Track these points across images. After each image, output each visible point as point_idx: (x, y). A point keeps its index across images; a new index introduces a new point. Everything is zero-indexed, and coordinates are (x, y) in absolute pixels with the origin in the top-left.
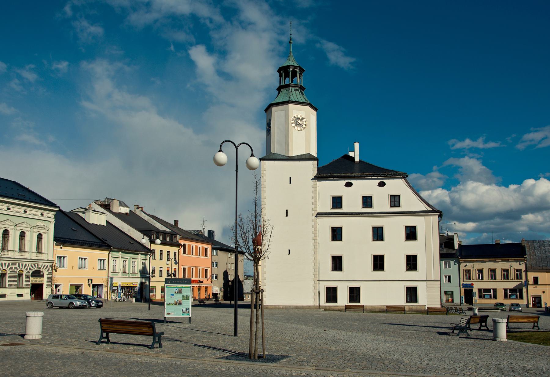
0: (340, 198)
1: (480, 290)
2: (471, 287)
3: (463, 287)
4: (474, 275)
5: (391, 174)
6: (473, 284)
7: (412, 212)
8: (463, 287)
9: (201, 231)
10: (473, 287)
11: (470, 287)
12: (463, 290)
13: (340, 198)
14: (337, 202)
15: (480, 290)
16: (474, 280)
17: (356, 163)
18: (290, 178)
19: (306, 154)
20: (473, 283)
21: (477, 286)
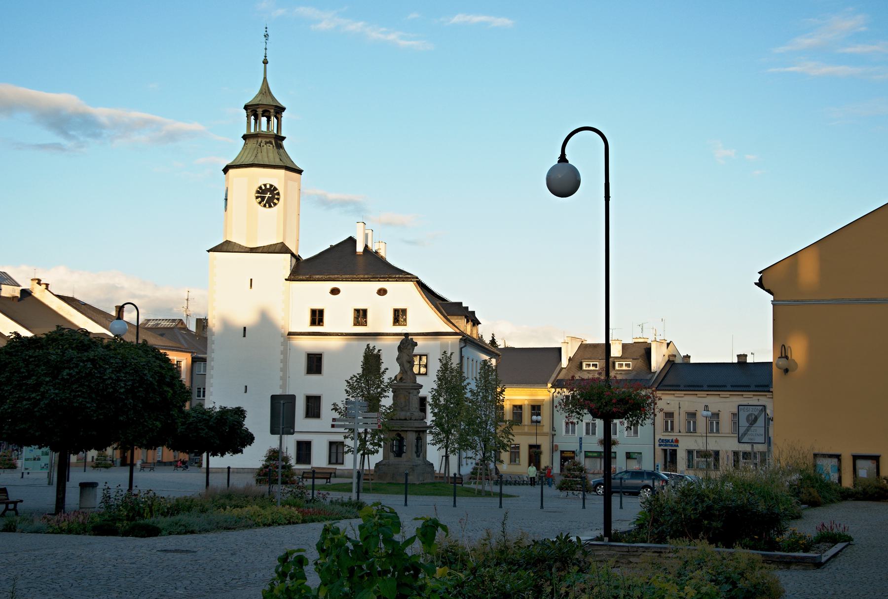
0: (321, 312)
1: (690, 452)
2: (675, 446)
3: (660, 445)
4: (680, 421)
5: (395, 278)
6: (677, 441)
7: (422, 334)
8: (660, 445)
9: (181, 320)
10: (677, 446)
11: (671, 446)
12: (659, 449)
13: (321, 312)
14: (317, 317)
15: (690, 452)
16: (680, 432)
17: (357, 253)
18: (251, 280)
19: (278, 243)
20: (679, 438)
21: (686, 444)
